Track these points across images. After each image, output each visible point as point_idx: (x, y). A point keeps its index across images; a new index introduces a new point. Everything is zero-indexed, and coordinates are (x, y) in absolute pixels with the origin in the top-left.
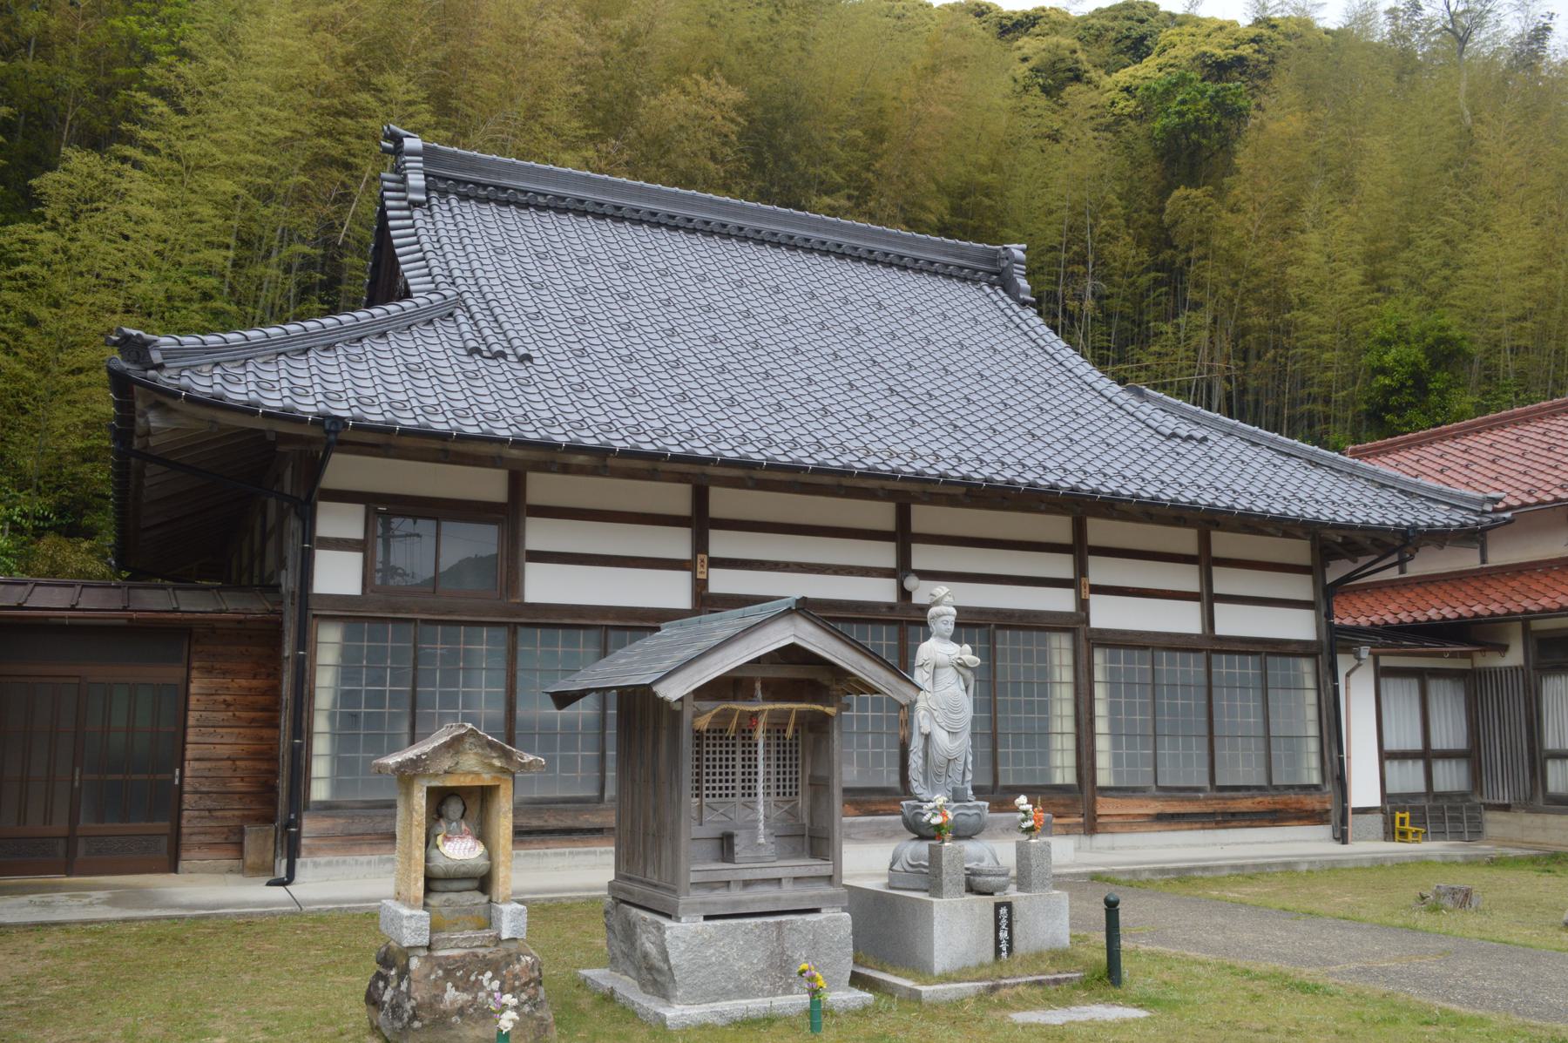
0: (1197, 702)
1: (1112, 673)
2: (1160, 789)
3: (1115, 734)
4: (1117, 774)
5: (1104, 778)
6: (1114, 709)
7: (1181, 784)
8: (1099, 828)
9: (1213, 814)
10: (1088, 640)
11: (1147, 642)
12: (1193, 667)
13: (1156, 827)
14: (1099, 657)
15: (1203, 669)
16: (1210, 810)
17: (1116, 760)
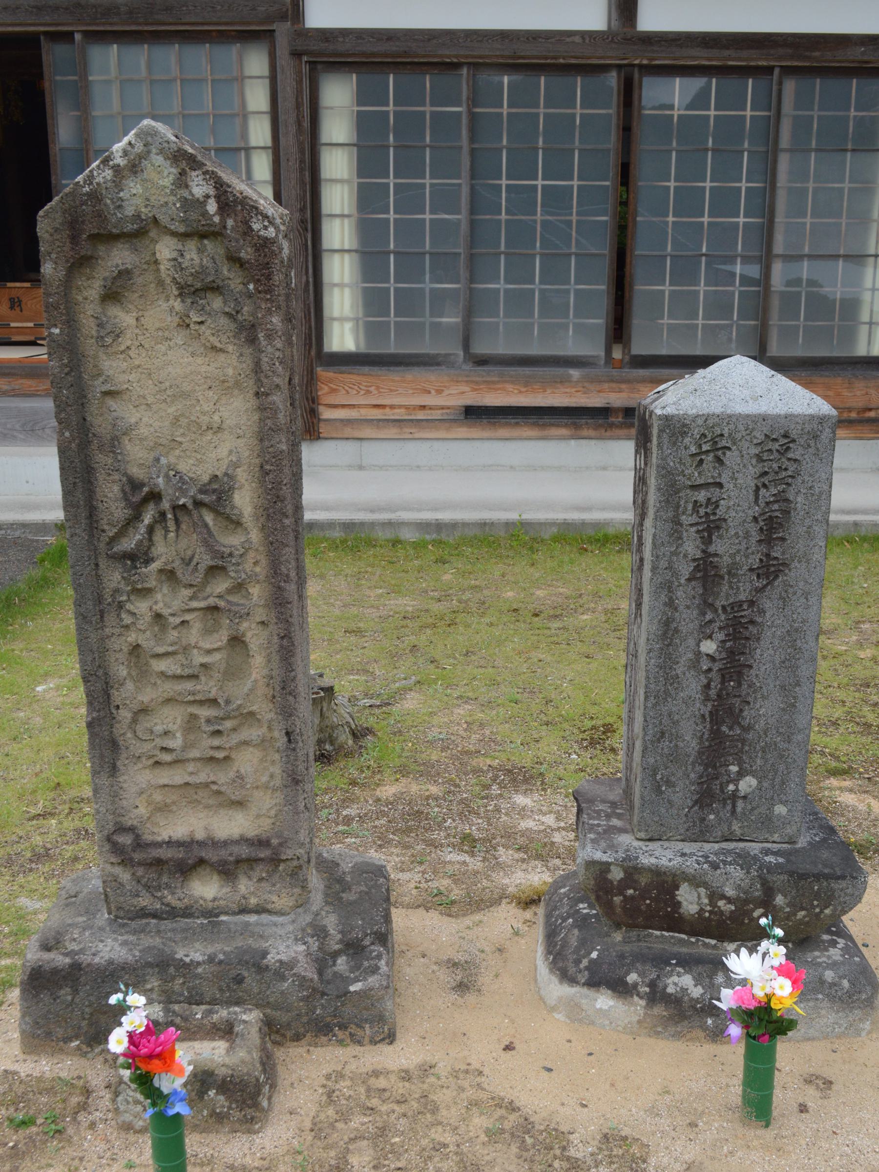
0: (584, 184)
1: (369, 132)
2: (482, 361)
3: (371, 257)
4: (372, 331)
5: (342, 338)
6: (368, 199)
7: (535, 350)
8: (323, 429)
9: (603, 413)
10: (296, 54)
11: (449, 54)
12: (588, 107)
13: (462, 431)
14: (338, 96)
15: (611, 111)
16: (595, 401)
17: (373, 302)
